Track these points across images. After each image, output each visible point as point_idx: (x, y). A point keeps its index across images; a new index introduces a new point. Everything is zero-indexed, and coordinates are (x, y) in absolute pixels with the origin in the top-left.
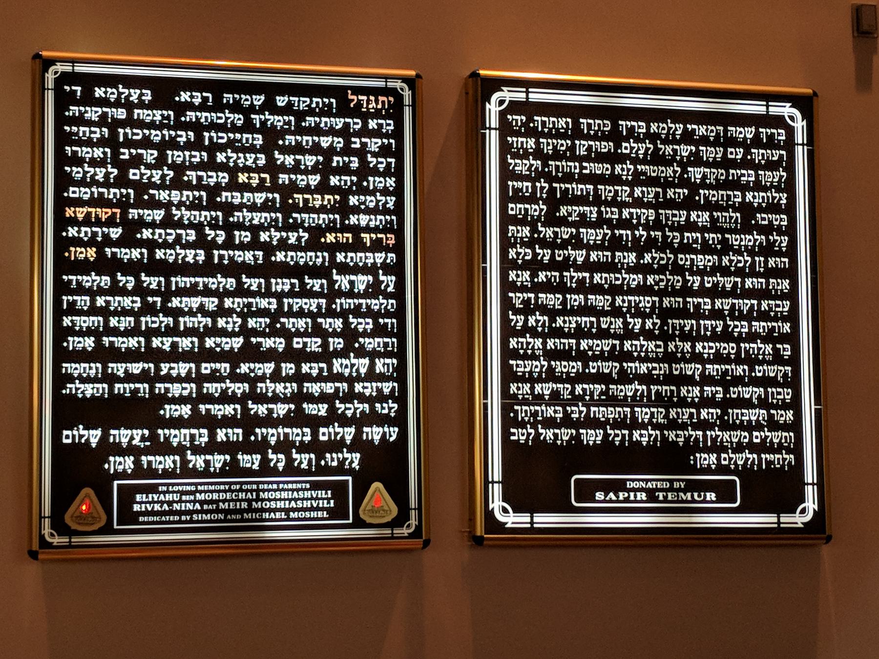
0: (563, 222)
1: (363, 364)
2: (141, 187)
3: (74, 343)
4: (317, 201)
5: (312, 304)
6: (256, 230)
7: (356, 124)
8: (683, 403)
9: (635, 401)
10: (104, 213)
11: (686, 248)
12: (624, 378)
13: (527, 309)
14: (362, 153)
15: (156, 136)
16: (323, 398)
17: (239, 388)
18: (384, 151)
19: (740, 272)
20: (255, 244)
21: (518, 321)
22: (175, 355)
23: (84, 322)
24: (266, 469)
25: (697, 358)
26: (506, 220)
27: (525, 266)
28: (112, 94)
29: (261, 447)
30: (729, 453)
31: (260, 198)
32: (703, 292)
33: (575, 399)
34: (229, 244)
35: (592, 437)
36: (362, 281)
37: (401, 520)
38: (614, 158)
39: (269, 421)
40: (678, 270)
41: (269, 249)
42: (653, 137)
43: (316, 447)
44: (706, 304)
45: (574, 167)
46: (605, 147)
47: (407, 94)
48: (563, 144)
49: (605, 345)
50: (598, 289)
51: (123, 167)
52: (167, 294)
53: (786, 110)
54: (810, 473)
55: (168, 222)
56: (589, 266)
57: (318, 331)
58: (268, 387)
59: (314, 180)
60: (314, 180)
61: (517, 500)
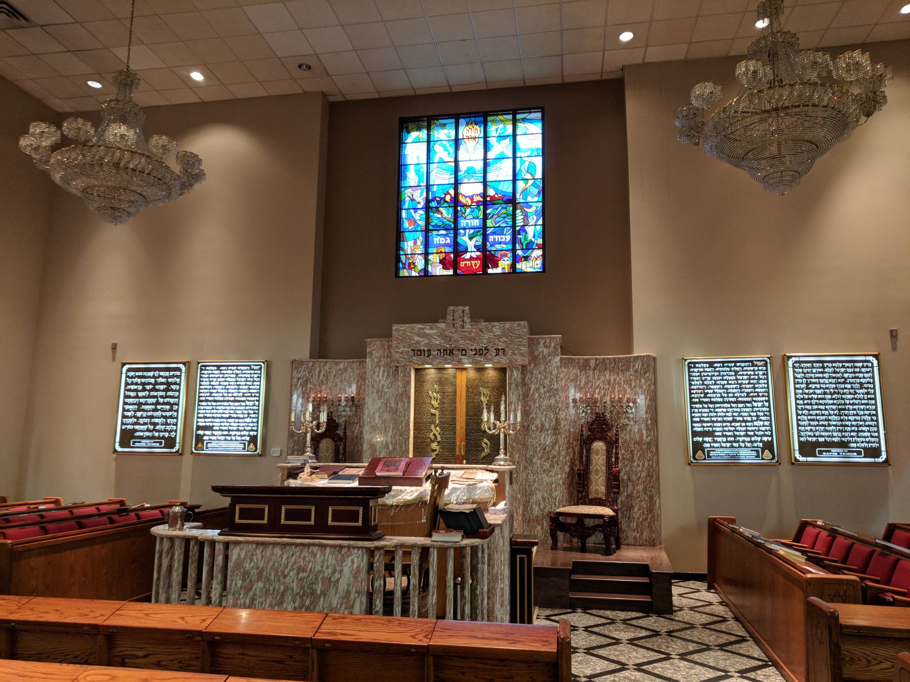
1: (761, 423)
2: (707, 385)
3: (695, 419)
4: (748, 386)
5: (748, 410)
7: (756, 368)
8: (846, 431)
9: (833, 431)
11: (844, 394)
12: (829, 425)
13: (802, 410)
17: (733, 429)
18: (764, 374)
19: (860, 399)
21: (800, 412)
22: (717, 422)
24: (740, 447)
25: (849, 420)
26: (796, 389)
28: (700, 365)
29: (738, 442)
30: (859, 443)
32: (850, 404)
33: (816, 431)
35: (821, 440)
36: (760, 404)
37: (773, 458)
38: (823, 373)
39: (740, 436)
40: (842, 399)
41: (737, 397)
42: (834, 367)
43: (751, 442)
44: (851, 407)
45: (813, 375)
46: (821, 370)
48: (809, 370)
49: (824, 418)
50: (821, 404)
52: (714, 408)
53: (871, 358)
54: (883, 448)
55: (714, 393)
56: (818, 399)
57: (750, 416)
61: (802, 453)
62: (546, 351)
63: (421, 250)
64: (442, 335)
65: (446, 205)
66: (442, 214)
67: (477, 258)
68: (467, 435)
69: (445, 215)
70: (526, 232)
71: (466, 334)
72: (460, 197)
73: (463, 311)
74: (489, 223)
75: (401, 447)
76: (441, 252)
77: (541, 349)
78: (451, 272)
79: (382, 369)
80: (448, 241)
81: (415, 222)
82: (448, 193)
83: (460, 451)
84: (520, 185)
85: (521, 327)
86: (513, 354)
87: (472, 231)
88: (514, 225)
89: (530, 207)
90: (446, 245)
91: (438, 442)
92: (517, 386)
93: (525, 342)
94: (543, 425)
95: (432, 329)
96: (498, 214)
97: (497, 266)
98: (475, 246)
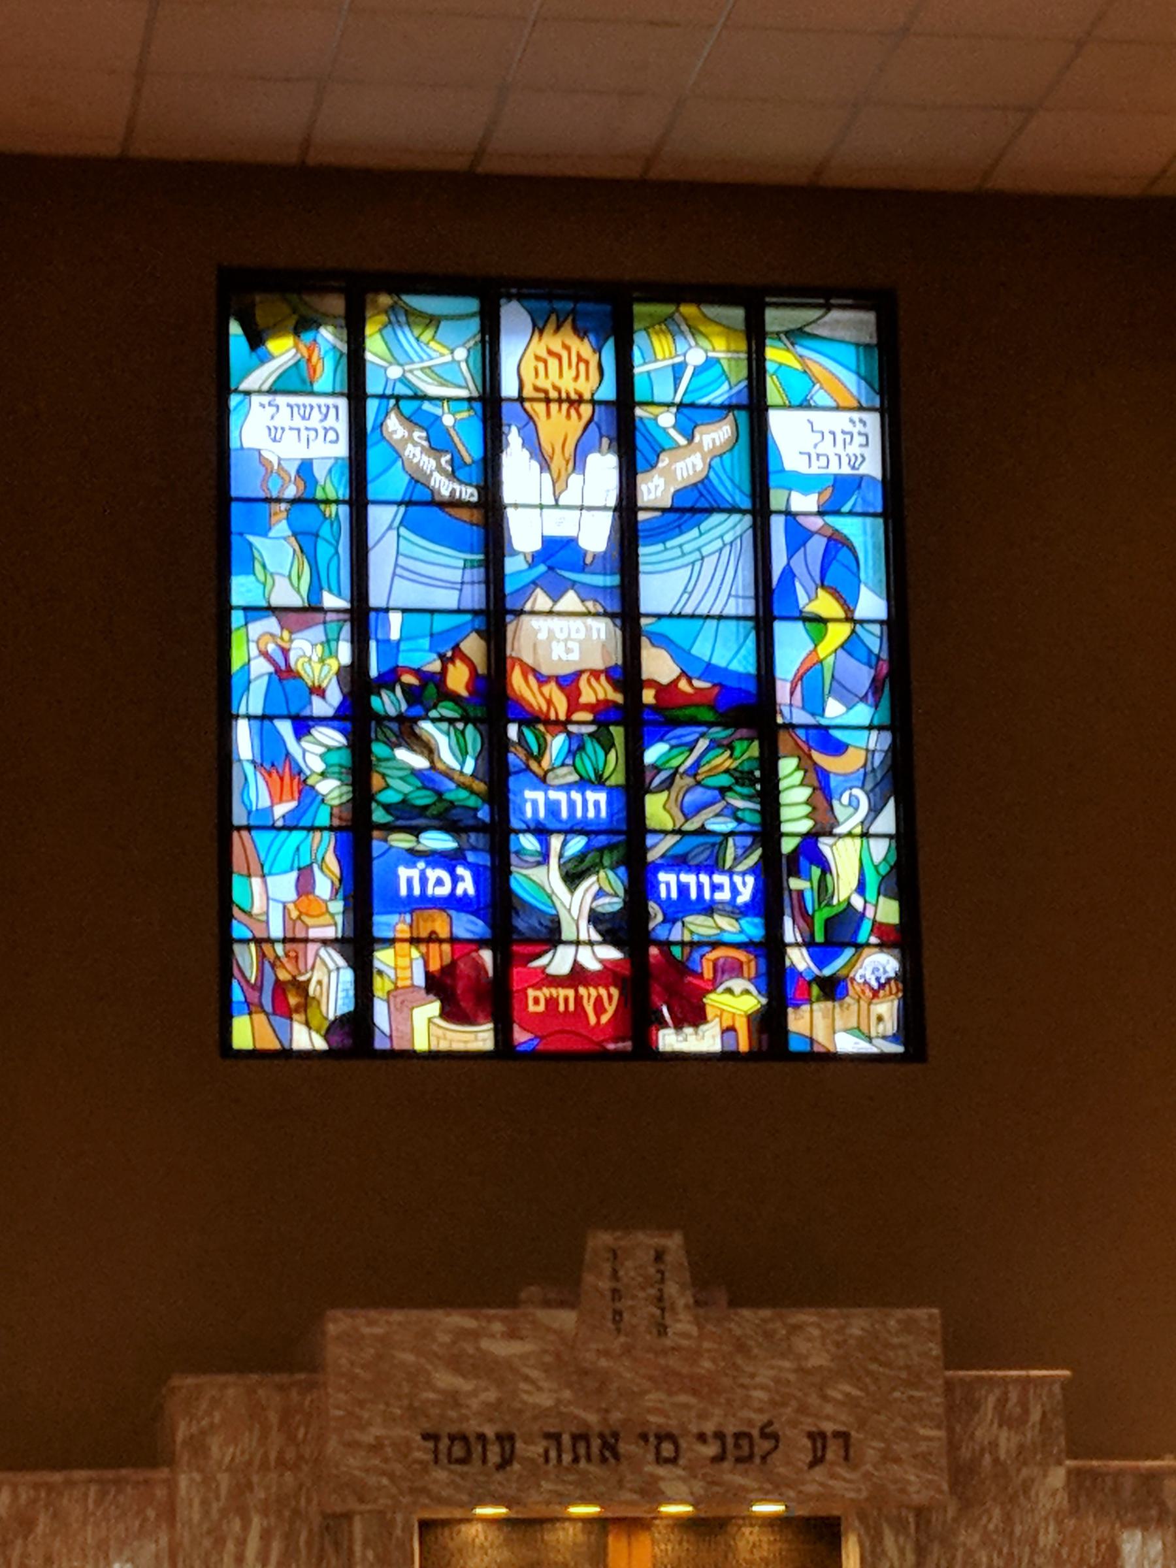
66: (429, 750)
67: (608, 975)
69: (447, 758)
70: (826, 869)
71: (673, 1361)
72: (517, 681)
73: (659, 1257)
74: (657, 810)
76: (433, 938)
80: (467, 886)
87: (577, 844)
89: (838, 748)
90: (453, 903)
95: (513, 1334)
97: (694, 1016)
98: (595, 918)
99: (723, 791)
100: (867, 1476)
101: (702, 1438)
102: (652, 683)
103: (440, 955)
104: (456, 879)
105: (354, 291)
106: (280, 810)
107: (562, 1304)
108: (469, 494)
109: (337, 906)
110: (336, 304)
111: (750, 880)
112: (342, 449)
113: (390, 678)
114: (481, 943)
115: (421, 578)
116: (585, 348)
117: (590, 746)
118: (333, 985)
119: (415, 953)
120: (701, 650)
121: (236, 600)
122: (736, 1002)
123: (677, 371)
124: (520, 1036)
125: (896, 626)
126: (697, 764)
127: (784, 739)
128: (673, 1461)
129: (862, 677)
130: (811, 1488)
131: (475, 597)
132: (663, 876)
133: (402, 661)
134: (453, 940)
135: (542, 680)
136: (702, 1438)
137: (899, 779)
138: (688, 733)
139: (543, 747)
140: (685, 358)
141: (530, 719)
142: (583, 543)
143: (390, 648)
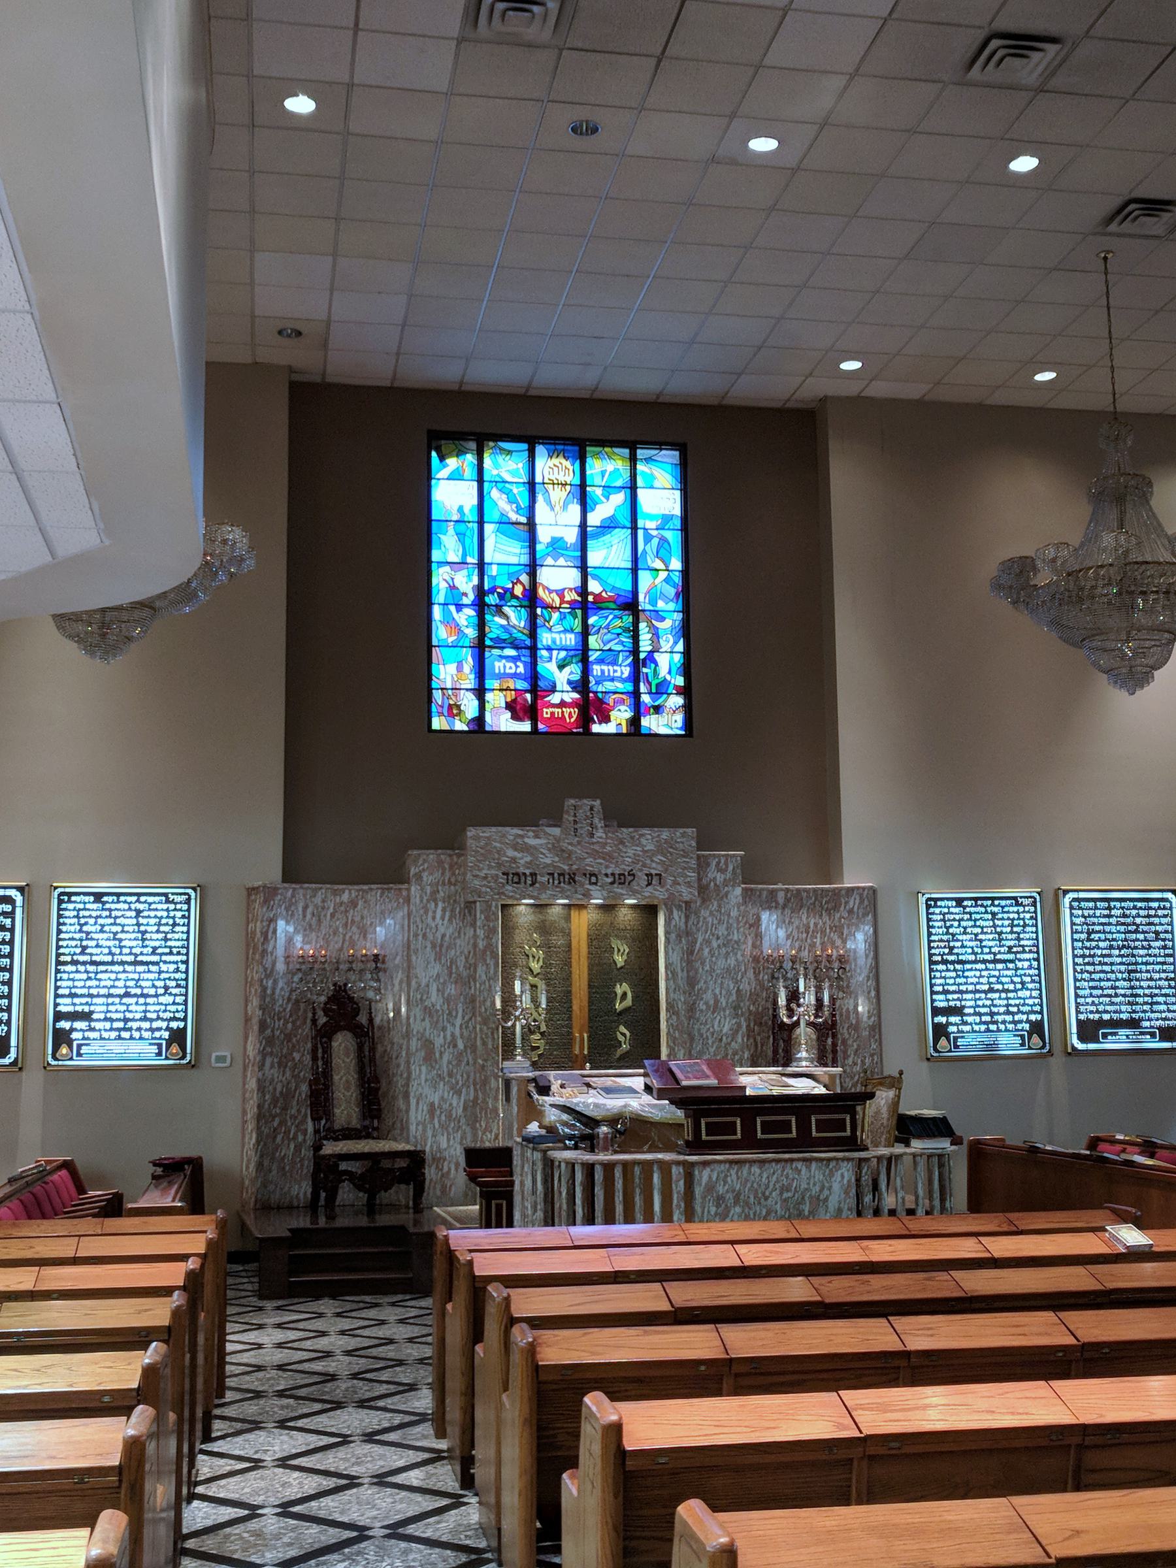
0: (1093, 940)
1: (1028, 993)
3: (936, 989)
4: (1010, 936)
6: (990, 947)
8: (1137, 1004)
9: (1121, 1004)
10: (942, 944)
11: (1136, 948)
12: (1116, 995)
13: (1082, 972)
14: (1023, 919)
15: (957, 917)
16: (1016, 1005)
17: (988, 1003)
19: (1155, 956)
20: (990, 953)
21: (1079, 976)
22: (967, 992)
23: (939, 981)
24: (999, 1030)
25: (1141, 987)
26: (1073, 940)
27: (1081, 956)
29: (996, 1023)
31: (991, 937)
32: (1142, 963)
33: (1100, 1003)
34: (982, 953)
35: (1106, 1017)
36: (1026, 964)
37: (1043, 1047)
38: (1109, 916)
40: (1133, 956)
41: (995, 954)
42: (1123, 908)
43: (1014, 1022)
44: (1144, 968)
45: (1096, 920)
46: (1106, 912)
47: (1038, 898)
48: (1091, 912)
49: (1109, 984)
50: (1106, 964)
51: (947, 928)
55: (963, 946)
56: (1103, 956)
57: (1012, 982)
58: (996, 1002)
59: (1009, 929)
60: (1009, 929)
62: (720, 878)
63: (470, 682)
64: (556, 849)
65: (514, 602)
66: (507, 618)
68: (590, 1019)
69: (514, 620)
71: (597, 847)
72: (541, 591)
73: (592, 809)
74: (593, 641)
75: (484, 1043)
76: (508, 689)
77: (714, 875)
78: (526, 726)
79: (440, 905)
80: (521, 669)
81: (459, 630)
82: (519, 581)
83: (582, 1048)
84: (645, 579)
85: (685, 837)
86: (676, 883)
87: (563, 654)
88: (635, 651)
89: (663, 619)
90: (515, 676)
91: (542, 1034)
92: (679, 936)
93: (693, 863)
94: (717, 1001)
96: (607, 627)
97: (606, 719)
98: (570, 682)
99: (618, 634)
100: (667, 890)
101: (606, 875)
102: (592, 593)
103: (511, 696)
104: (517, 667)
105: (481, 440)
106: (451, 639)
107: (555, 826)
108: (524, 520)
109: (472, 676)
110: (473, 445)
111: (628, 669)
112: (475, 501)
113: (493, 590)
114: (526, 691)
115: (505, 553)
116: (567, 464)
117: (569, 617)
118: (470, 707)
119: (501, 694)
120: (611, 581)
121: (434, 559)
122: (620, 717)
123: (603, 473)
124: (541, 726)
125: (685, 573)
126: (608, 624)
127: (641, 615)
128: (595, 884)
129: (672, 592)
130: (647, 894)
131: (525, 559)
132: (595, 667)
133: (498, 584)
134: (515, 690)
135: (551, 592)
136: (606, 875)
137: (686, 630)
138: (605, 613)
139: (550, 618)
140: (606, 467)
141: (546, 606)
142: (566, 539)
143: (494, 578)
